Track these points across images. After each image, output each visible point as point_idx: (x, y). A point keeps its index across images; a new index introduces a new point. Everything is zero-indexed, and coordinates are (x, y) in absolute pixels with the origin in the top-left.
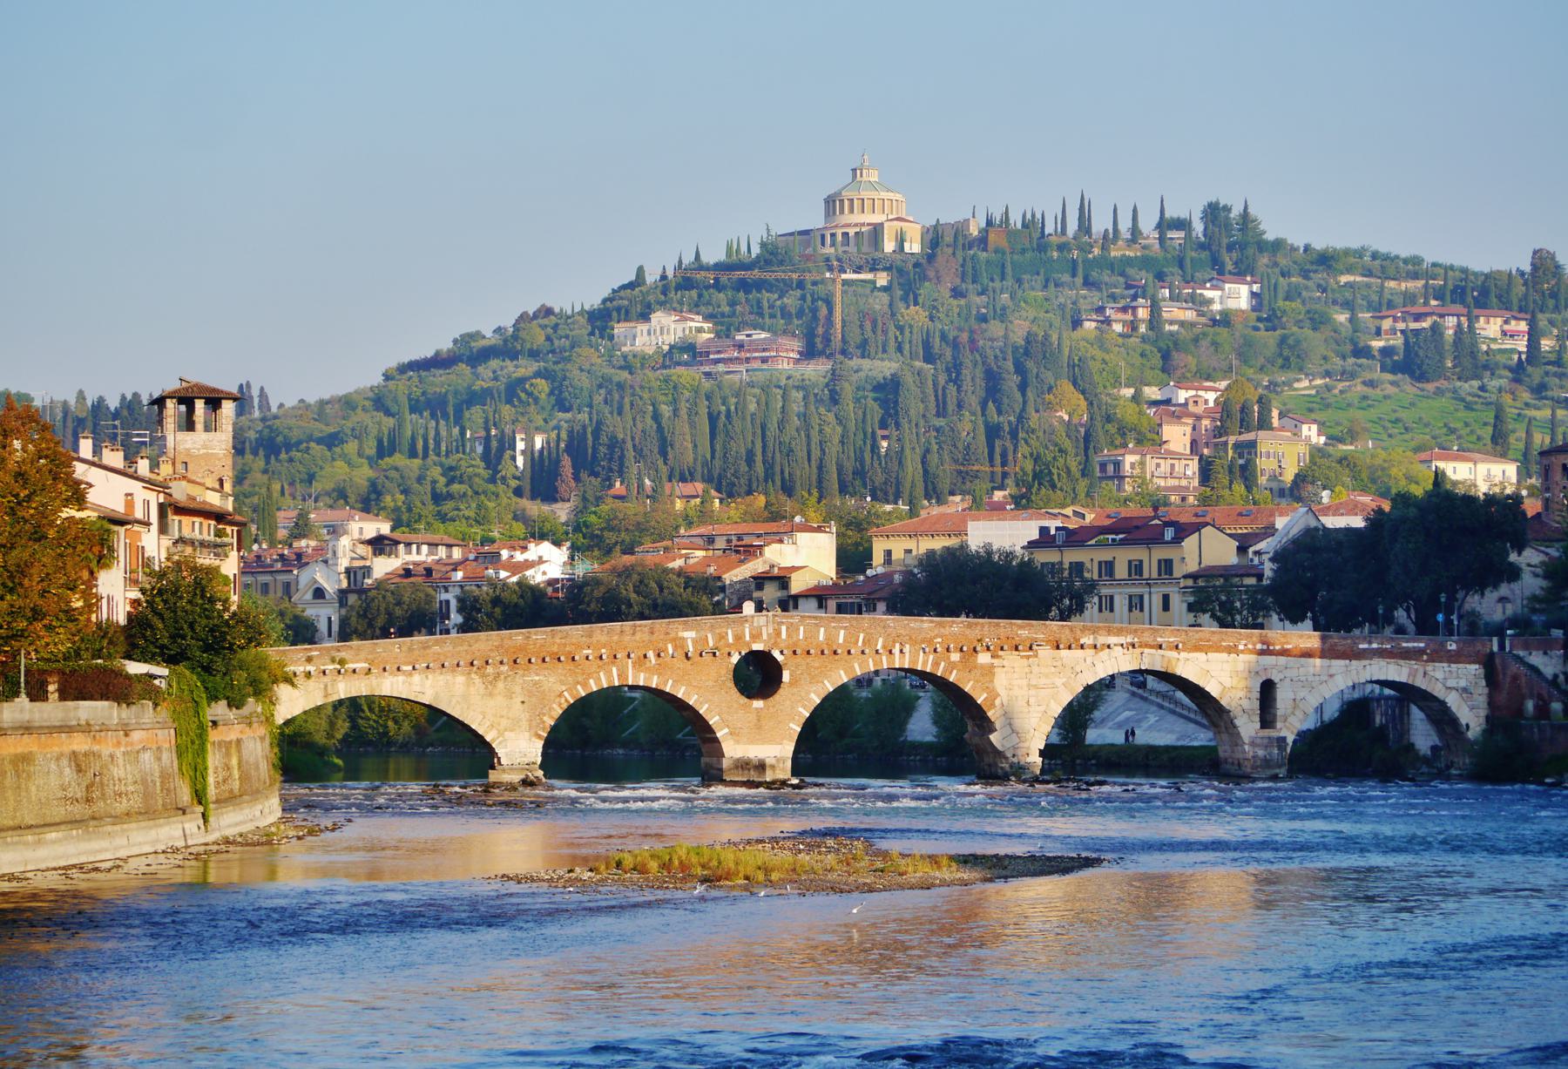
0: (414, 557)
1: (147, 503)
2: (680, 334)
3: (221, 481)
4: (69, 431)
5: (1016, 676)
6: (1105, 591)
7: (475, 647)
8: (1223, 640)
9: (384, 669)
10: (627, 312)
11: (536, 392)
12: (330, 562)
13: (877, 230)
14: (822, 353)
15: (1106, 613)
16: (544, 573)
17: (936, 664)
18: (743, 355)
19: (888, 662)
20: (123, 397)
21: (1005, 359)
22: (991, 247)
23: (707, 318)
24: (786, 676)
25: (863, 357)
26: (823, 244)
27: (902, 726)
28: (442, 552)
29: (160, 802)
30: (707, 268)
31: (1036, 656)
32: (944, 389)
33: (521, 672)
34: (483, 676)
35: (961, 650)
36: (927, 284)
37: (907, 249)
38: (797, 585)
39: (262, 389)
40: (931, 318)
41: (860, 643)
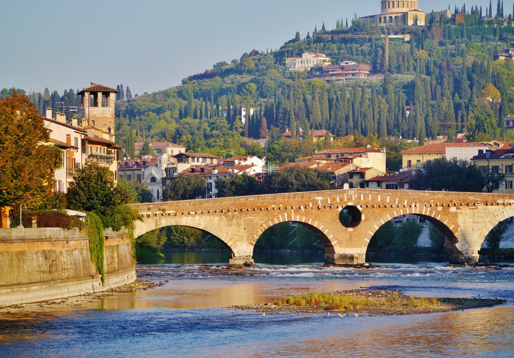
0: (196, 163)
1: (76, 139)
2: (315, 63)
3: (109, 129)
4: (41, 106)
5: (467, 217)
6: (508, 179)
7: (223, 203)
9: (183, 214)
10: (292, 53)
11: (250, 89)
12: (158, 165)
13: (405, 16)
14: (379, 71)
15: (509, 189)
16: (254, 171)
17: (431, 212)
18: (344, 72)
19: (409, 211)
20: (66, 91)
21: (463, 74)
22: (457, 23)
23: (328, 55)
24: (363, 217)
25: (398, 73)
26: (380, 22)
27: (416, 239)
28: (208, 161)
29: (82, 273)
30: (328, 33)
32: (435, 87)
33: (244, 215)
34: (227, 217)
35: (443, 205)
36: (427, 40)
37: (419, 24)
38: (368, 176)
39: (128, 88)
40: (430, 55)
41: (397, 203)
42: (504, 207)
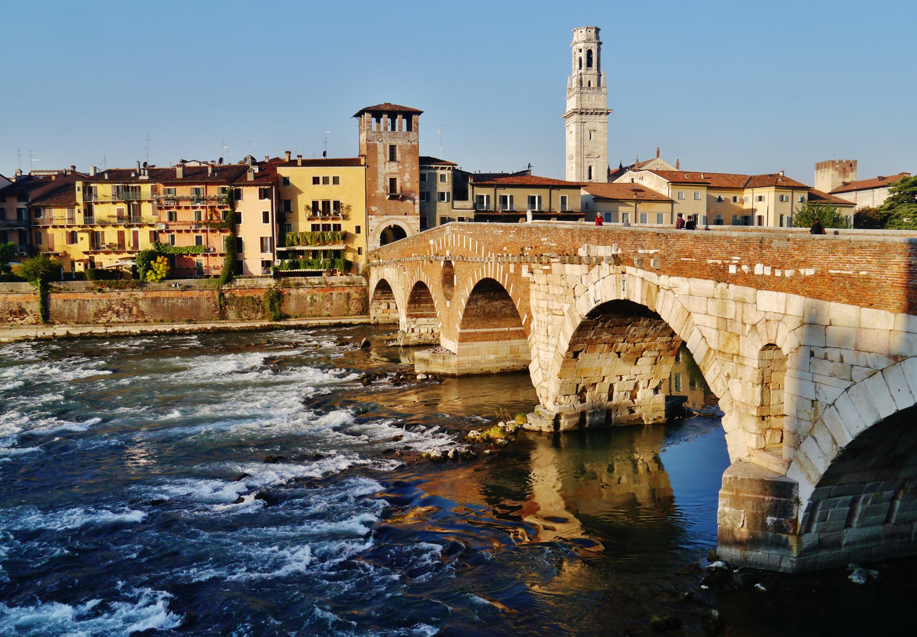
8: (709, 255)
42: (589, 270)
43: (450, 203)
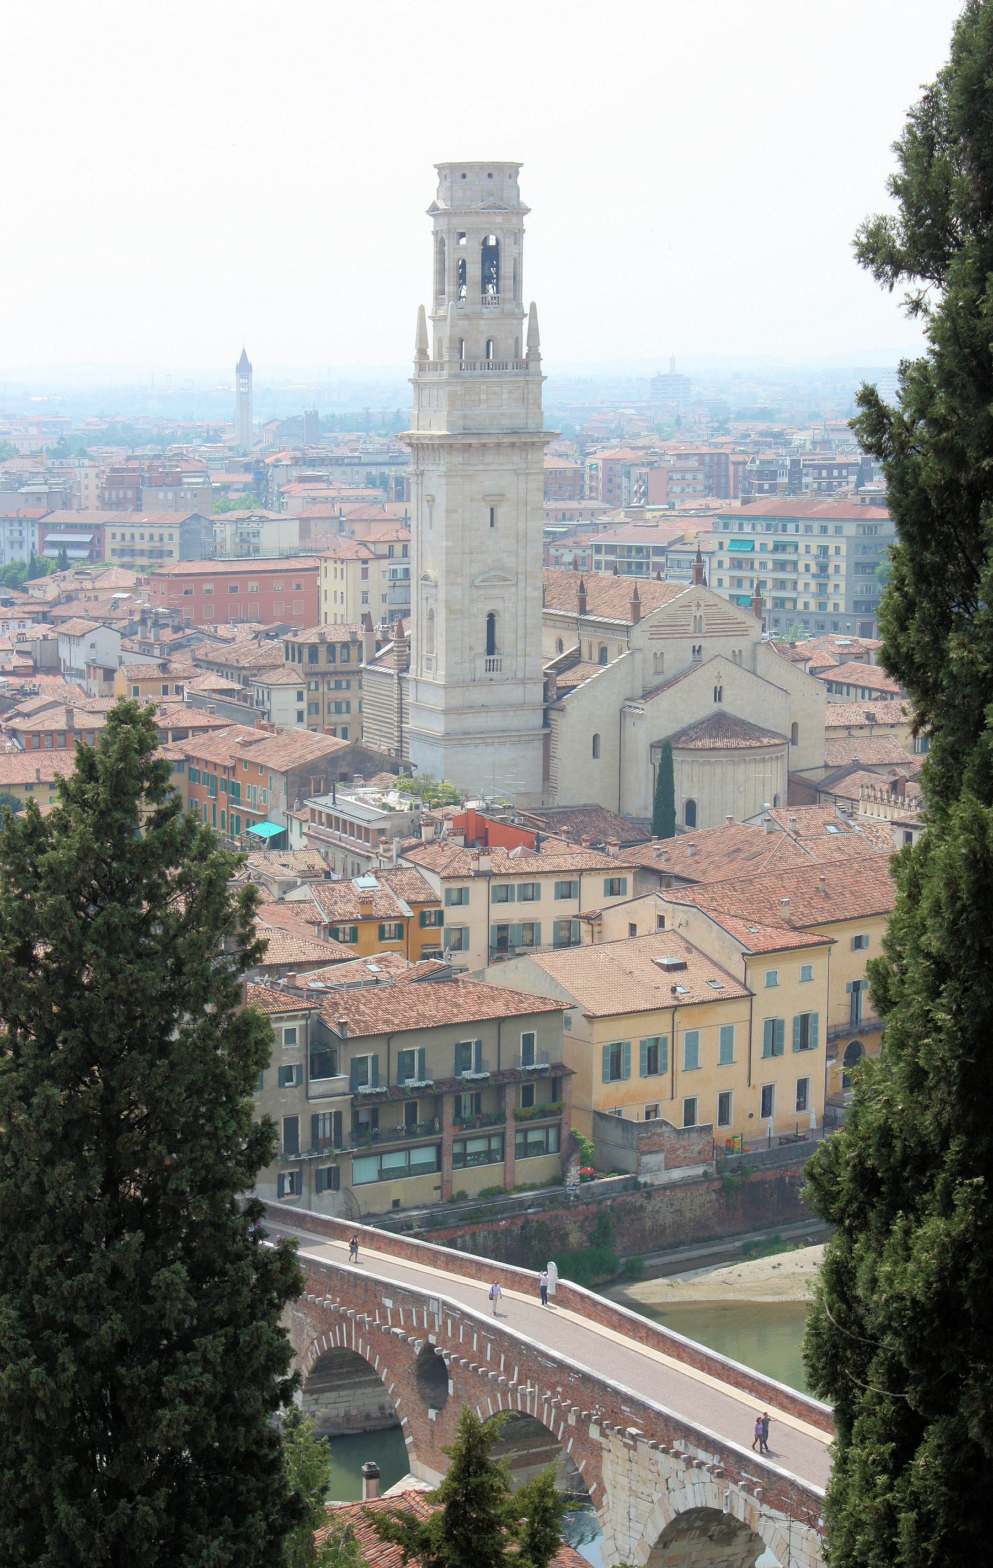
5: (620, 1469)
31: (635, 1448)
42: (687, 1468)
43: (304, 1085)
